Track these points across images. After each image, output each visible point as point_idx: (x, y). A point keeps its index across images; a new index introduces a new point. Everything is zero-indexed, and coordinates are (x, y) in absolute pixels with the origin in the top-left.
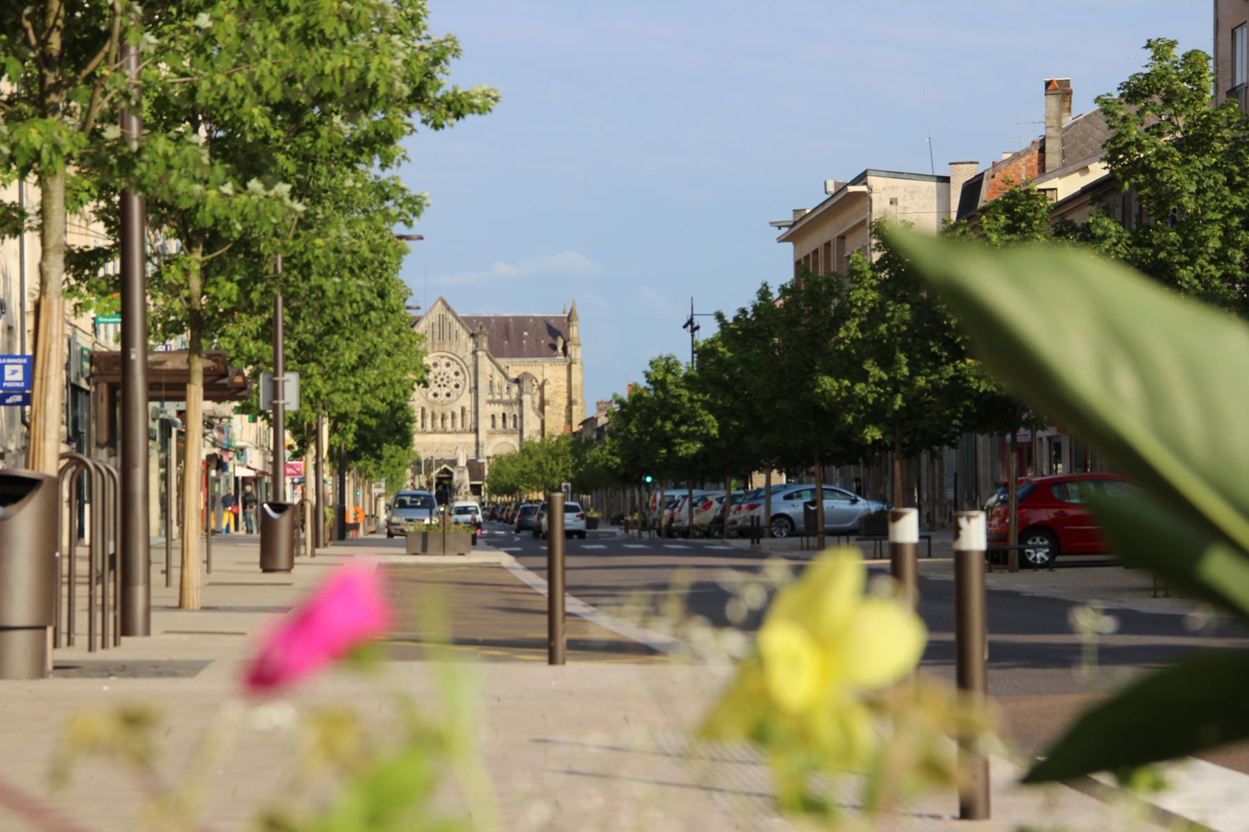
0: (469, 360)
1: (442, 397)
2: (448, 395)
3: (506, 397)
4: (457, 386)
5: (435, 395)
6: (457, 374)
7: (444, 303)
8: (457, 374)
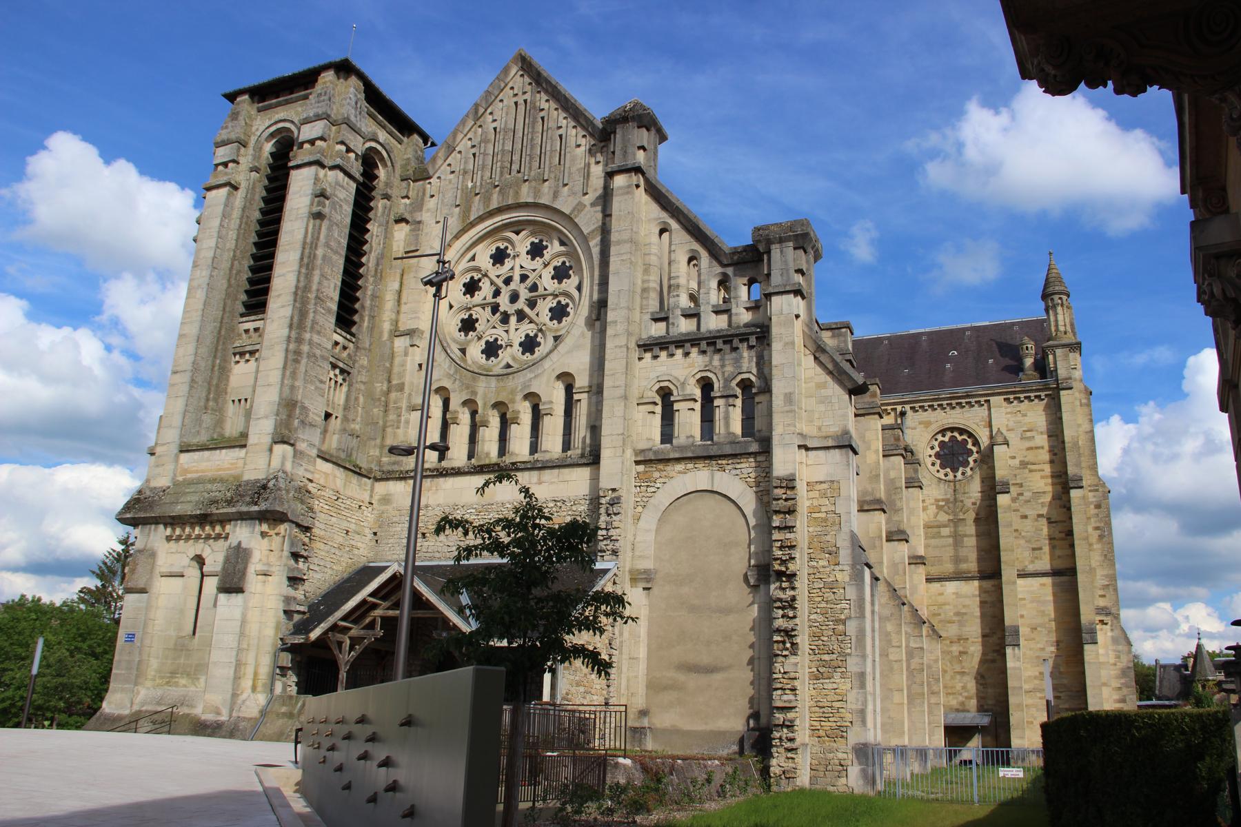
0: (589, 220)
2: (529, 345)
3: (714, 323)
4: (559, 313)
5: (492, 350)
6: (561, 274)
7: (527, 66)
8: (561, 274)
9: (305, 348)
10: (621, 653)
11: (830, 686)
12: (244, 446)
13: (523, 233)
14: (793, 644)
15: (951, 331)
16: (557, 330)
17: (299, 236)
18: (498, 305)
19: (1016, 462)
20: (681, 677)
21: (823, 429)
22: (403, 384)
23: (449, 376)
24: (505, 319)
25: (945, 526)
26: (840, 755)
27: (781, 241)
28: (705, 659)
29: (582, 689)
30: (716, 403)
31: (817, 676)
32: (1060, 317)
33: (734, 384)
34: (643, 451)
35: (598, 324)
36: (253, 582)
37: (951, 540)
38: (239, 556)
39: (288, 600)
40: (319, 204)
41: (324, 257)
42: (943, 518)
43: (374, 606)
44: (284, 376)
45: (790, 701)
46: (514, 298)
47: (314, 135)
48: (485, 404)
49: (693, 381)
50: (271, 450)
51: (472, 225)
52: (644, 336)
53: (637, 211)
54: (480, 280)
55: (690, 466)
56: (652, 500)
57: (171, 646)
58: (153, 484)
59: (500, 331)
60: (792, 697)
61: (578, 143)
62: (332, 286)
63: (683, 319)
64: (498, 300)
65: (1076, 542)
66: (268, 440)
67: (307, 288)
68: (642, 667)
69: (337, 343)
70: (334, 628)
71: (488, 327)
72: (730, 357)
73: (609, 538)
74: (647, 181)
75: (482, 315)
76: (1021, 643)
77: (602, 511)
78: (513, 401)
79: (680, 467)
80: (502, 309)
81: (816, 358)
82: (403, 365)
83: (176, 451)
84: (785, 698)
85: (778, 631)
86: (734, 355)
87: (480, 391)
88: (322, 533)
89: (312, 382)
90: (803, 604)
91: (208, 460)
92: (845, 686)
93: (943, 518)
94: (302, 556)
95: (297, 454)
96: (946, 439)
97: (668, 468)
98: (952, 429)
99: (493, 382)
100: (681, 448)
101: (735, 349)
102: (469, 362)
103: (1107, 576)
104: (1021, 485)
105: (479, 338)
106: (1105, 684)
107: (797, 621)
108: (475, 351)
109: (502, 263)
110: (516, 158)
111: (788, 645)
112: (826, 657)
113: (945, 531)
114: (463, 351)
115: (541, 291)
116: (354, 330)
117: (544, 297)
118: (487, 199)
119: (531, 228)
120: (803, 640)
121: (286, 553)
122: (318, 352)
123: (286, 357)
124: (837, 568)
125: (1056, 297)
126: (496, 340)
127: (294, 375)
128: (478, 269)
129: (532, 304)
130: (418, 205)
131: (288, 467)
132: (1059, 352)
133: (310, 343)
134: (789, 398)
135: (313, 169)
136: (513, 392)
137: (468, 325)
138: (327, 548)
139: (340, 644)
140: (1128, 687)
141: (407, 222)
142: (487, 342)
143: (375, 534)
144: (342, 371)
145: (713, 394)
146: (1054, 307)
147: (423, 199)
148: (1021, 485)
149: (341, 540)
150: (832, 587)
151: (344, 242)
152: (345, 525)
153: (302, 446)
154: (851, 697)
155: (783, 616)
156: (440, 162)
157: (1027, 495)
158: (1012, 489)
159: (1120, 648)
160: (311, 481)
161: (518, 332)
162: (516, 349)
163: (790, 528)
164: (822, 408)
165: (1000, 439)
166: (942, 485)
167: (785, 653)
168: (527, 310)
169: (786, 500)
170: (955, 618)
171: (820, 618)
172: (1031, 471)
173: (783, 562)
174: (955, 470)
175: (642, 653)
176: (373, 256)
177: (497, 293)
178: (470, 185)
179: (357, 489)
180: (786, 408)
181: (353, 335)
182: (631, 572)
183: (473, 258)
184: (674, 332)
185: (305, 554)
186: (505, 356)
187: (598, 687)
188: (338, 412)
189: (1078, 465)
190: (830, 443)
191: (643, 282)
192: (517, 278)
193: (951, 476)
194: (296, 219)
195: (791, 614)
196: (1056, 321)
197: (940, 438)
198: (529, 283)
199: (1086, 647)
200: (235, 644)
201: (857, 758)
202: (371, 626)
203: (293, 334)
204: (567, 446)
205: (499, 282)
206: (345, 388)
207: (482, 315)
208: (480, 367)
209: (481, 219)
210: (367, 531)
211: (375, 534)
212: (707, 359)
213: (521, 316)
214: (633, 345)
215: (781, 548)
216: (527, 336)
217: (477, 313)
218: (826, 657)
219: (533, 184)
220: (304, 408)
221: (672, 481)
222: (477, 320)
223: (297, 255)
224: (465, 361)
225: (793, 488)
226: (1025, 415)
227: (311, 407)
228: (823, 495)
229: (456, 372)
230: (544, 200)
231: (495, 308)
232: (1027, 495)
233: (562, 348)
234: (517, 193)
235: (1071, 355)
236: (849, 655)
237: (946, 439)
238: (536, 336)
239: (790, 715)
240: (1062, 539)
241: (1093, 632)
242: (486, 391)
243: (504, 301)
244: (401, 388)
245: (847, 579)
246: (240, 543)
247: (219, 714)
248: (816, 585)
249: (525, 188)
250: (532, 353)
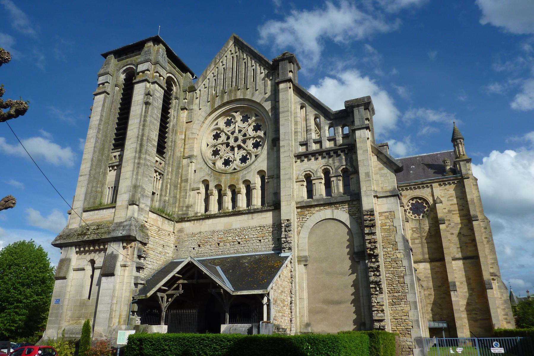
1: (237, 164)
2: (244, 160)
3: (328, 145)
4: (256, 145)
5: (227, 162)
9: (142, 161)
10: (296, 296)
11: (400, 309)
12: (114, 207)
13: (238, 113)
14: (380, 288)
15: (410, 158)
16: (256, 152)
17: (139, 112)
18: (229, 143)
19: (446, 210)
20: (325, 307)
21: (384, 188)
22: (188, 179)
23: (208, 175)
24: (233, 149)
25: (417, 239)
26: (408, 343)
27: (358, 106)
28: (336, 298)
29: (281, 314)
30: (332, 179)
31: (393, 304)
32: (461, 149)
33: (340, 170)
34: (299, 202)
35: (275, 148)
36: (118, 270)
37: (420, 245)
38: (114, 258)
39: (136, 278)
40: (147, 98)
41: (150, 121)
42: (416, 235)
43: (179, 278)
44: (133, 174)
45: (382, 317)
46: (236, 139)
47: (144, 69)
48: (225, 187)
49: (320, 171)
50: (127, 208)
51: (216, 110)
52: (297, 152)
53: (289, 99)
54: (220, 133)
55: (322, 208)
56: (305, 224)
57: (78, 304)
58: (70, 227)
59: (230, 154)
60: (382, 314)
61: (261, 72)
62: (155, 134)
63: (314, 144)
64: (229, 141)
65: (478, 244)
66: (126, 203)
67: (143, 135)
68: (306, 303)
69: (157, 161)
70: (160, 290)
71: (225, 153)
72: (337, 160)
73: (287, 242)
74: (294, 85)
75: (222, 149)
76: (458, 289)
77: (283, 230)
78: (238, 184)
79: (317, 209)
80: (231, 145)
81: (377, 157)
82: (188, 171)
83: (81, 211)
84: (379, 315)
85: (372, 282)
86: (338, 158)
87: (223, 181)
88: (152, 246)
89: (146, 177)
90: (382, 269)
91: (97, 214)
92: (407, 308)
93: (416, 235)
94: (143, 257)
95: (140, 210)
96: (414, 202)
97: (312, 209)
98: (416, 198)
99: (229, 176)
100: (317, 200)
101: (338, 155)
102: (217, 168)
103: (493, 259)
104: (449, 220)
105: (221, 158)
106: (498, 307)
107: (381, 277)
108: (220, 164)
109: (230, 126)
110: (234, 80)
111: (378, 289)
112: (396, 294)
113: (417, 241)
114: (214, 164)
115: (248, 136)
116: (164, 156)
117: (250, 139)
118: (222, 97)
119: (242, 110)
120: (384, 286)
121: (136, 256)
122: (149, 164)
123: (134, 166)
124: (397, 251)
125: (458, 141)
126: (229, 158)
127: (137, 174)
128: (219, 129)
129: (244, 142)
130: (191, 102)
131: (136, 215)
132: (461, 163)
133: (145, 159)
134: (367, 175)
135: (144, 84)
136: (238, 180)
137: (216, 153)
138: (154, 253)
139: (162, 298)
140: (508, 308)
141: (187, 109)
142: (225, 159)
143: (176, 247)
144: (160, 174)
145: (330, 175)
146: (458, 145)
147: (193, 99)
148: (449, 220)
149: (161, 250)
150: (395, 261)
151: (160, 116)
152: (162, 243)
153: (142, 206)
154: (411, 314)
155: (374, 275)
156: (200, 83)
157: (453, 224)
158: (446, 222)
159: (502, 291)
160: (146, 222)
161: (239, 154)
162: (238, 162)
163: (374, 234)
164: (383, 179)
165: (438, 201)
166: (414, 222)
167: (376, 293)
168: (242, 144)
169: (370, 220)
170: (425, 279)
171: (391, 276)
172: (453, 214)
173: (371, 249)
174: (419, 215)
175: (305, 295)
176: (171, 124)
177: (228, 138)
178: (214, 92)
179: (168, 226)
180: (367, 179)
181: (164, 158)
182: (298, 257)
183: (217, 124)
184: (310, 149)
185: (144, 256)
186: (232, 166)
187: (287, 313)
188: (158, 192)
189: (475, 210)
190: (388, 194)
191: (295, 129)
192: (237, 131)
193: (417, 218)
194: (137, 105)
195: (378, 274)
196: (459, 150)
197: (411, 202)
198: (242, 133)
199: (488, 290)
200: (110, 301)
201: (418, 344)
202: (177, 288)
203: (137, 155)
204: (263, 203)
205: (229, 134)
206: (161, 182)
207: (222, 149)
208: (222, 170)
209: (220, 107)
210: (172, 245)
211: (176, 247)
212: (326, 160)
213: (240, 147)
214: (292, 155)
215: (370, 243)
216: (243, 155)
217: (219, 147)
218: (396, 294)
219: (243, 90)
220: (143, 189)
221: (314, 215)
222: (220, 150)
223: (138, 120)
224: (215, 168)
225: (373, 215)
226: (448, 190)
227: (146, 188)
228: (387, 218)
229: (211, 173)
230: (248, 97)
231: (228, 145)
232: (453, 224)
233: (259, 159)
234: (235, 95)
235: (467, 164)
236: (408, 293)
237: (414, 202)
238: (246, 155)
239: (382, 324)
240: (470, 243)
241: (490, 284)
242: (225, 181)
243: (231, 141)
244: (186, 181)
245: (403, 256)
246: (113, 252)
247: (102, 337)
248: (388, 260)
249: (239, 93)
250: (245, 163)
